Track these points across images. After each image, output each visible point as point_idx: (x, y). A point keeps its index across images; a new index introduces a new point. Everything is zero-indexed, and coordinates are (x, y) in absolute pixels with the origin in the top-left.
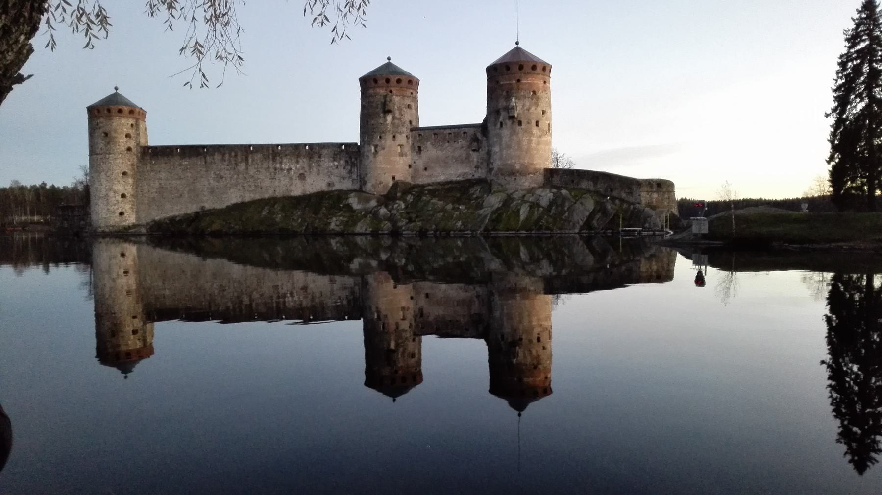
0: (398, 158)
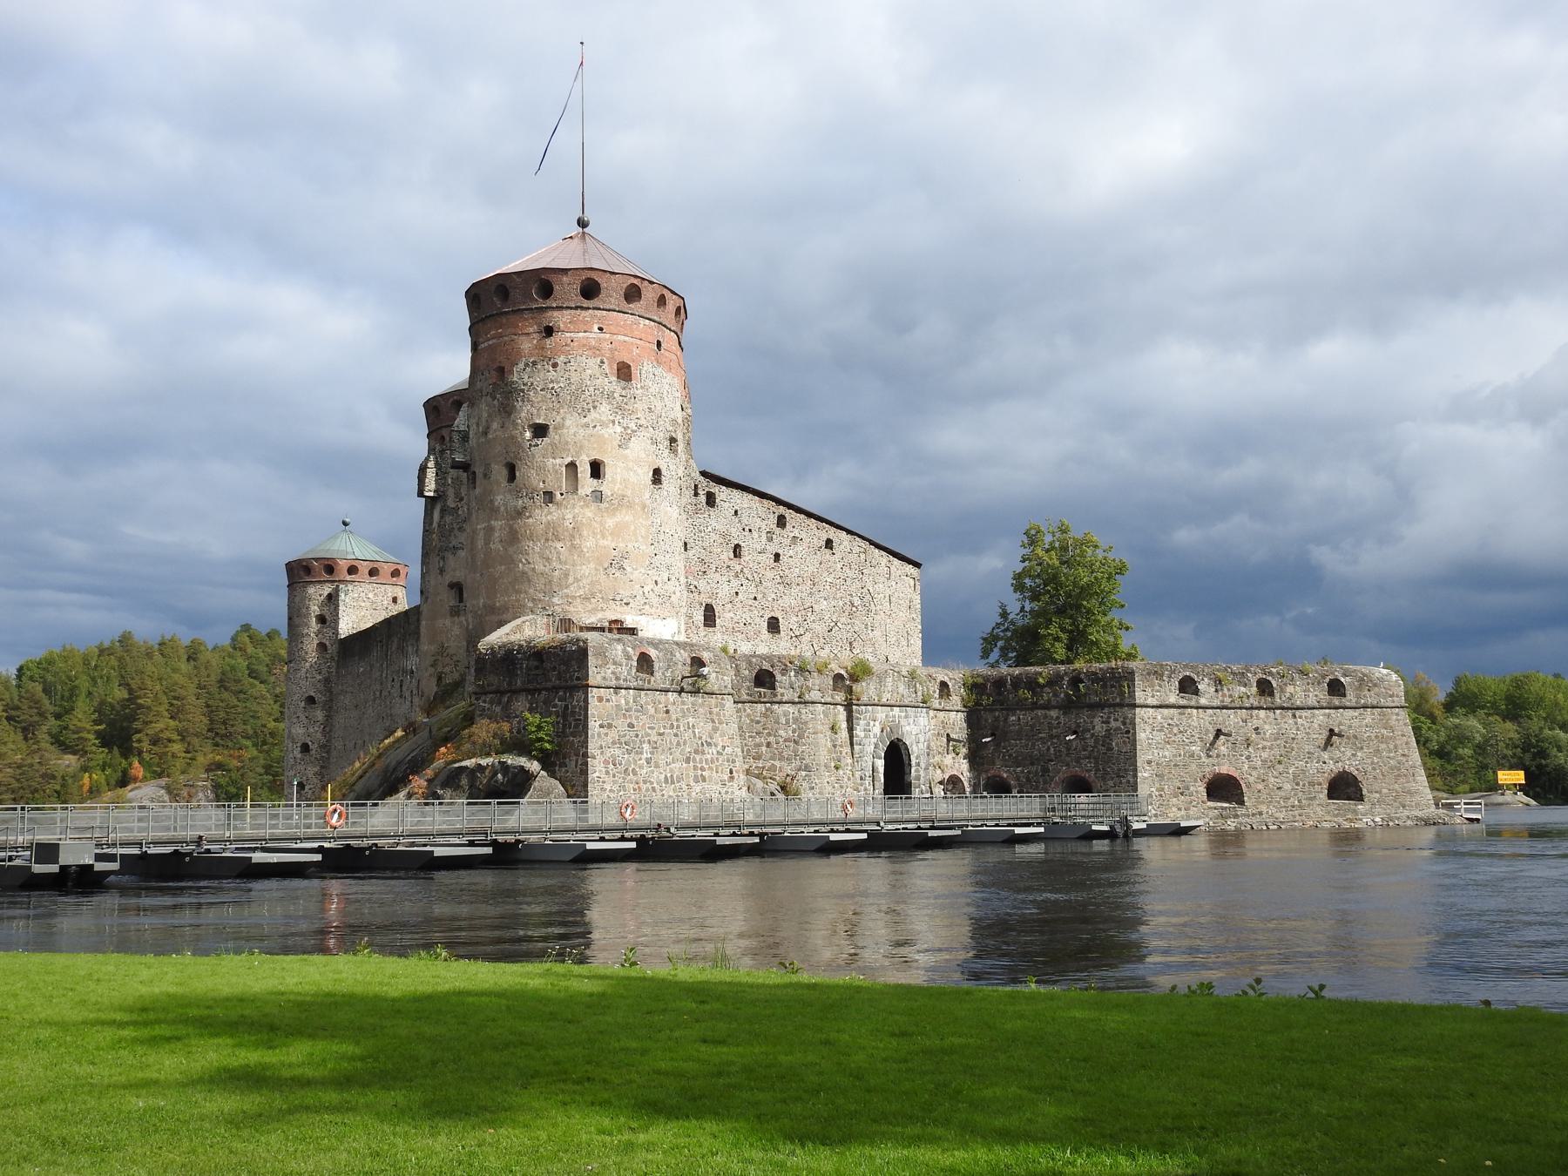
0: (448, 622)
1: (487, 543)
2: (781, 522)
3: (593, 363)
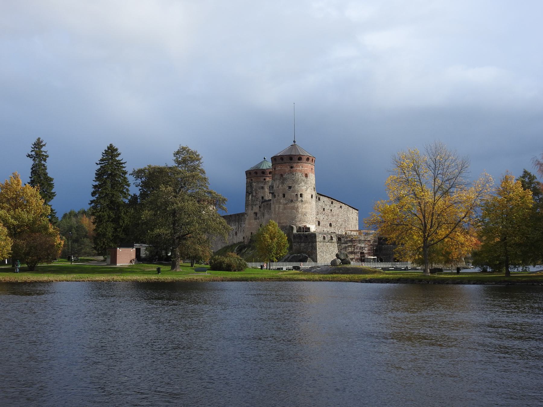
1: (279, 209)
2: (332, 203)
3: (300, 174)
